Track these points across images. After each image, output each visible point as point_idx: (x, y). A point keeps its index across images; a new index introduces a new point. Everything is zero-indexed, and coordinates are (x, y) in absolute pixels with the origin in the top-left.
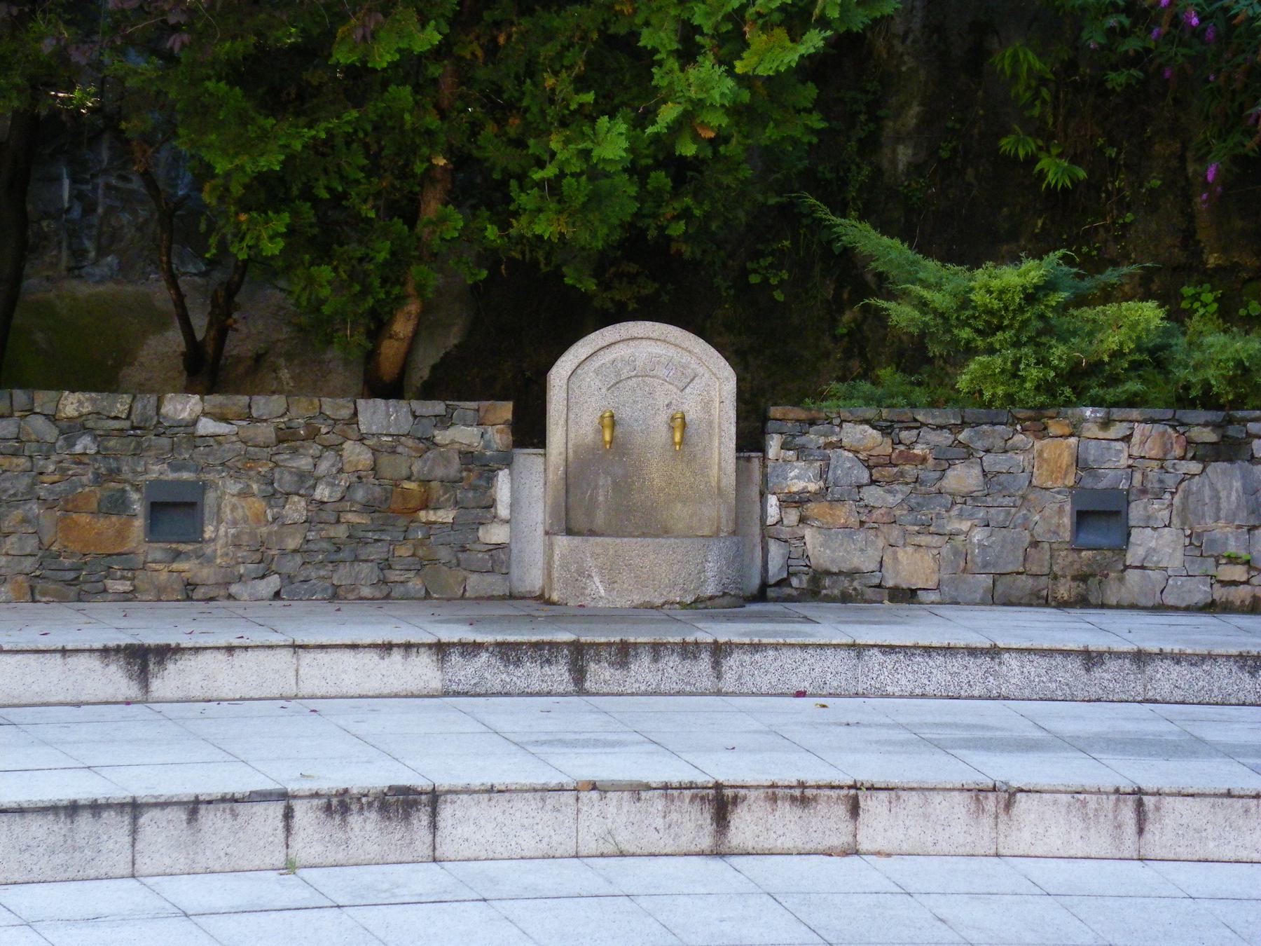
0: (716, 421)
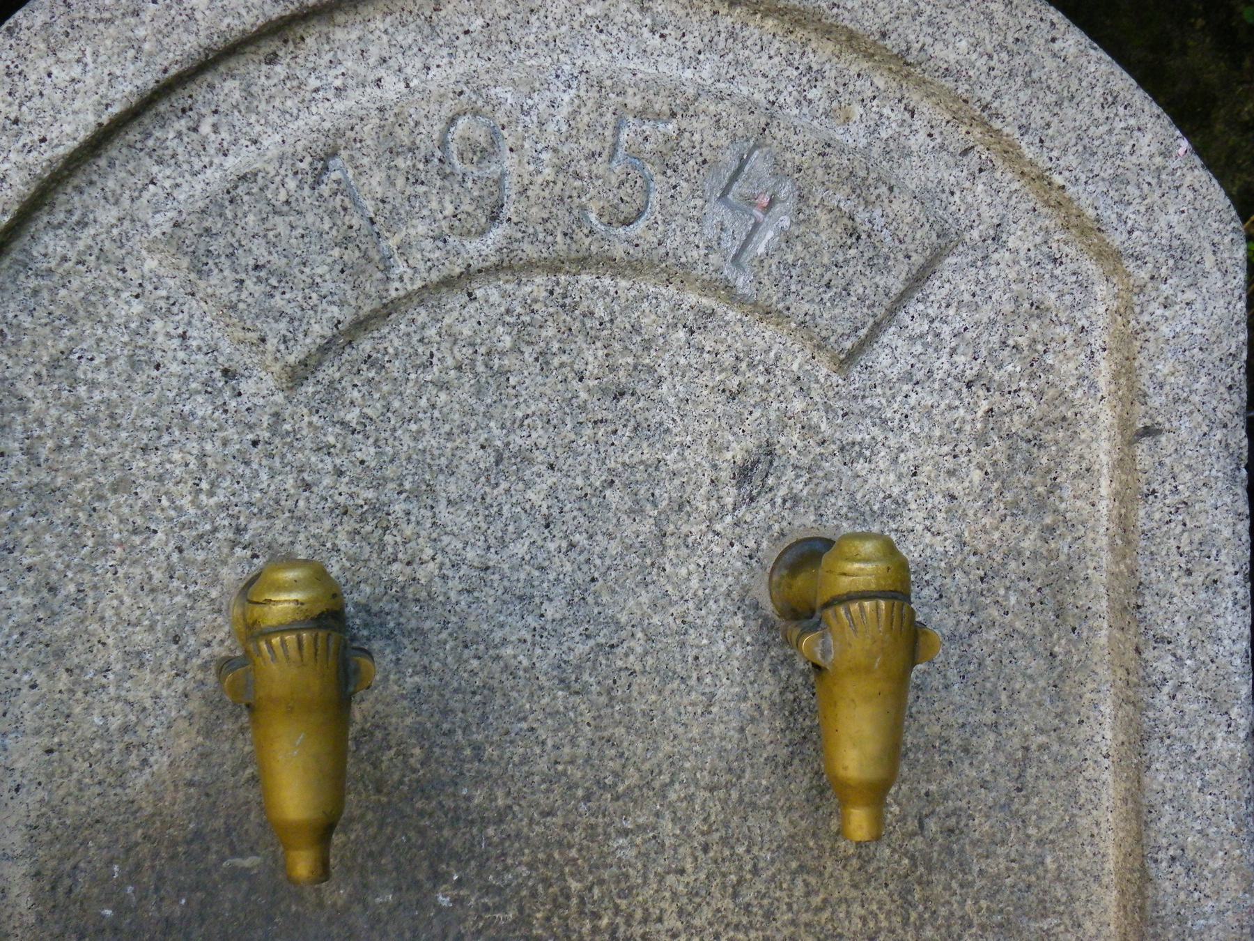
0: (1100, 568)
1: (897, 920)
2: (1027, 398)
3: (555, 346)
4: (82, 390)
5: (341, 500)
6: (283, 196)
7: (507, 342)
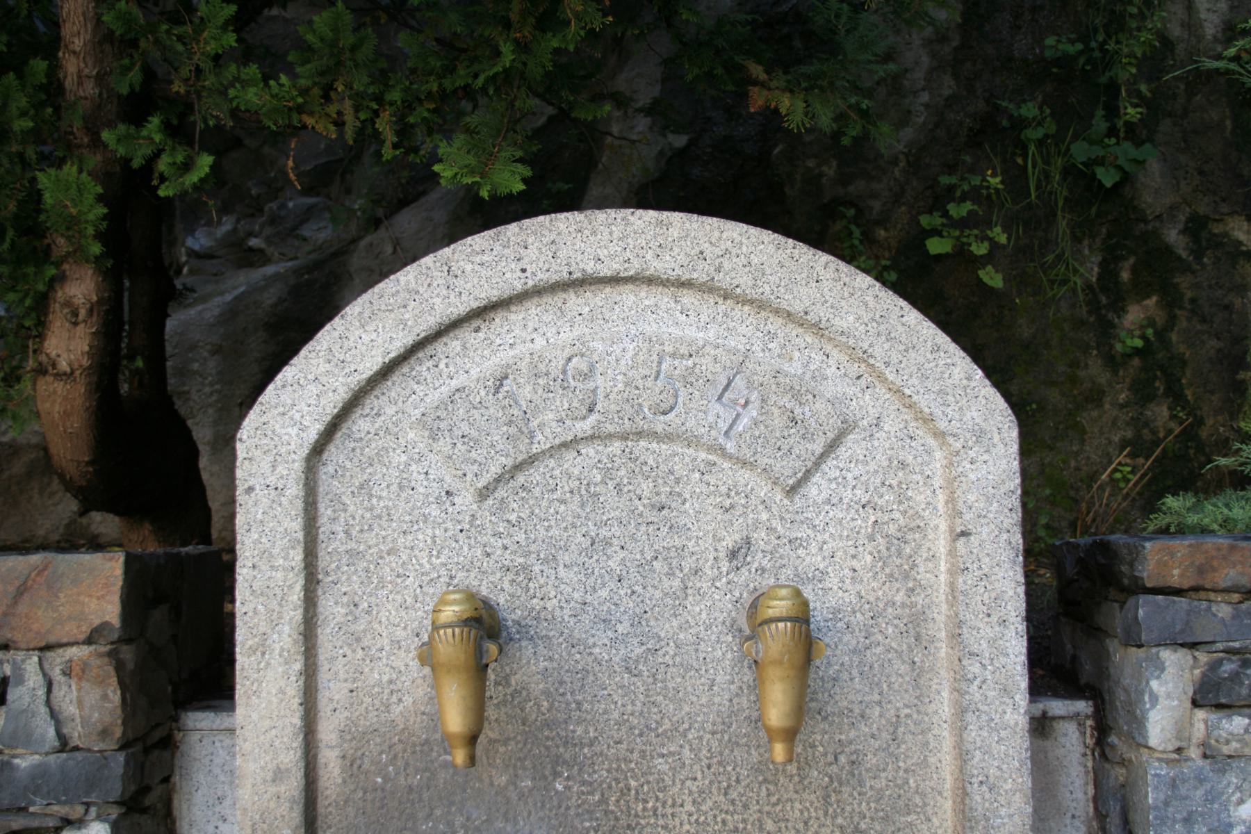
0: (940, 615)
1: (821, 813)
2: (897, 515)
3: (625, 481)
4: (374, 501)
5: (506, 563)
6: (478, 399)
7: (599, 478)
